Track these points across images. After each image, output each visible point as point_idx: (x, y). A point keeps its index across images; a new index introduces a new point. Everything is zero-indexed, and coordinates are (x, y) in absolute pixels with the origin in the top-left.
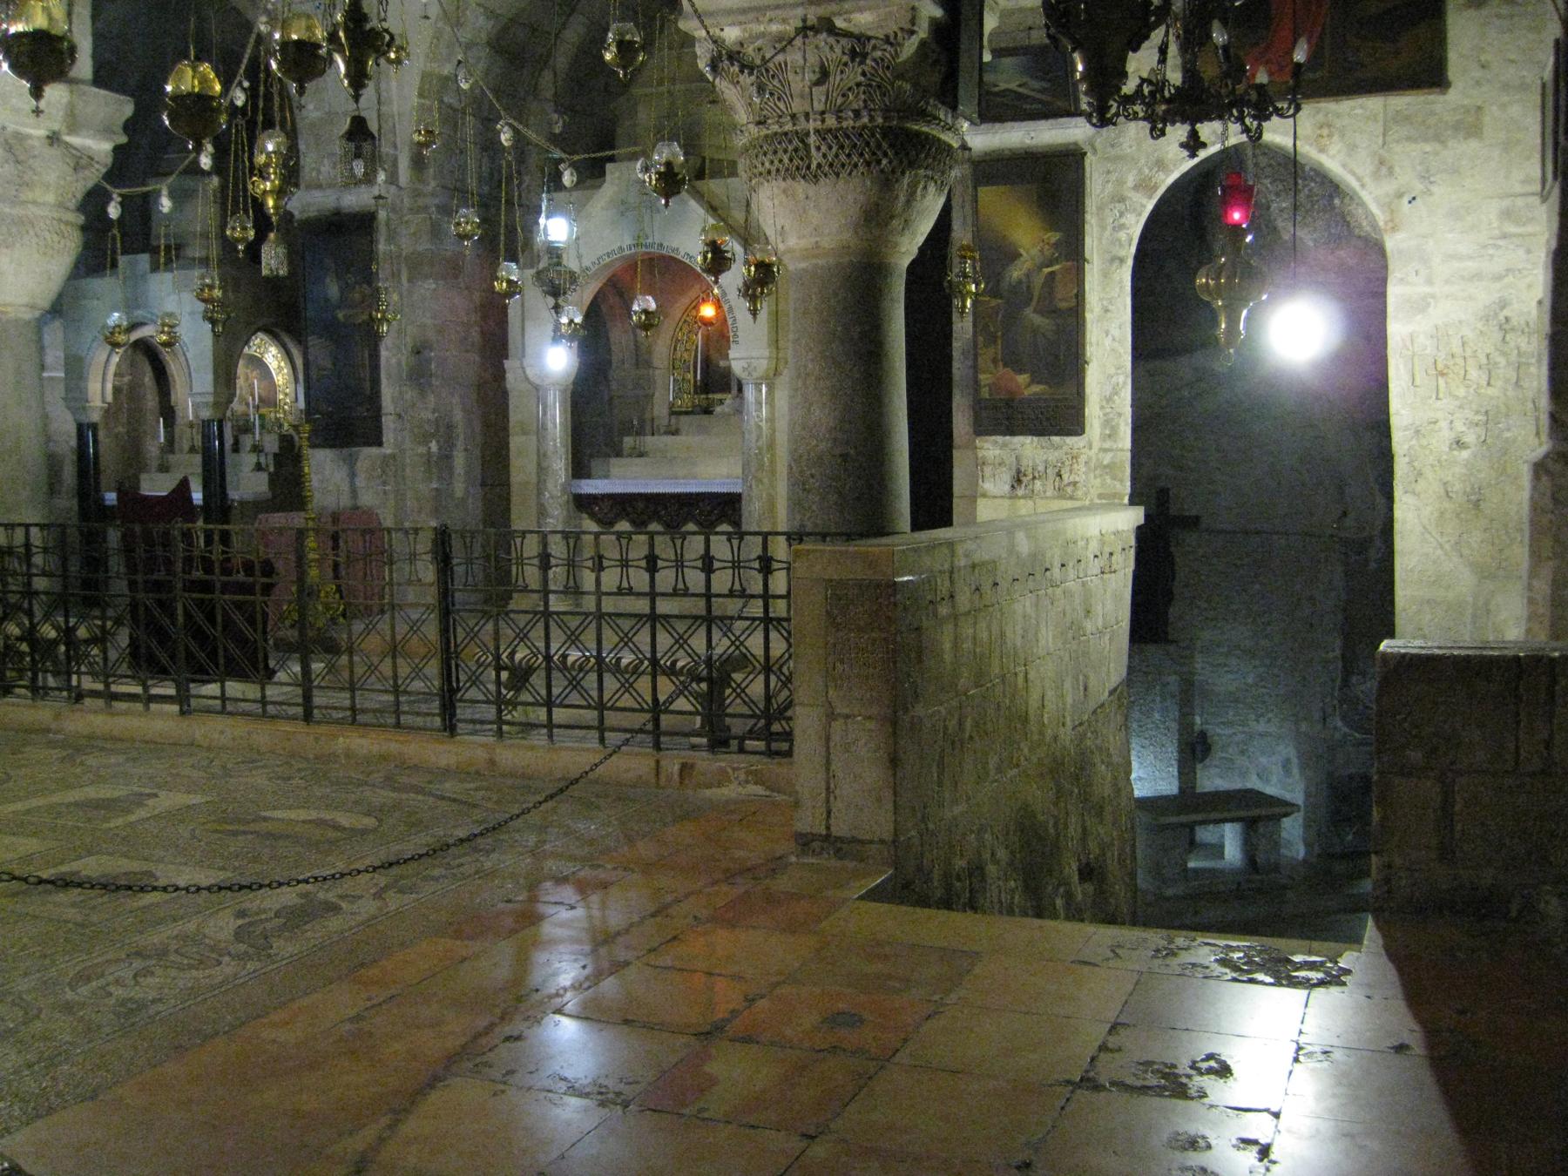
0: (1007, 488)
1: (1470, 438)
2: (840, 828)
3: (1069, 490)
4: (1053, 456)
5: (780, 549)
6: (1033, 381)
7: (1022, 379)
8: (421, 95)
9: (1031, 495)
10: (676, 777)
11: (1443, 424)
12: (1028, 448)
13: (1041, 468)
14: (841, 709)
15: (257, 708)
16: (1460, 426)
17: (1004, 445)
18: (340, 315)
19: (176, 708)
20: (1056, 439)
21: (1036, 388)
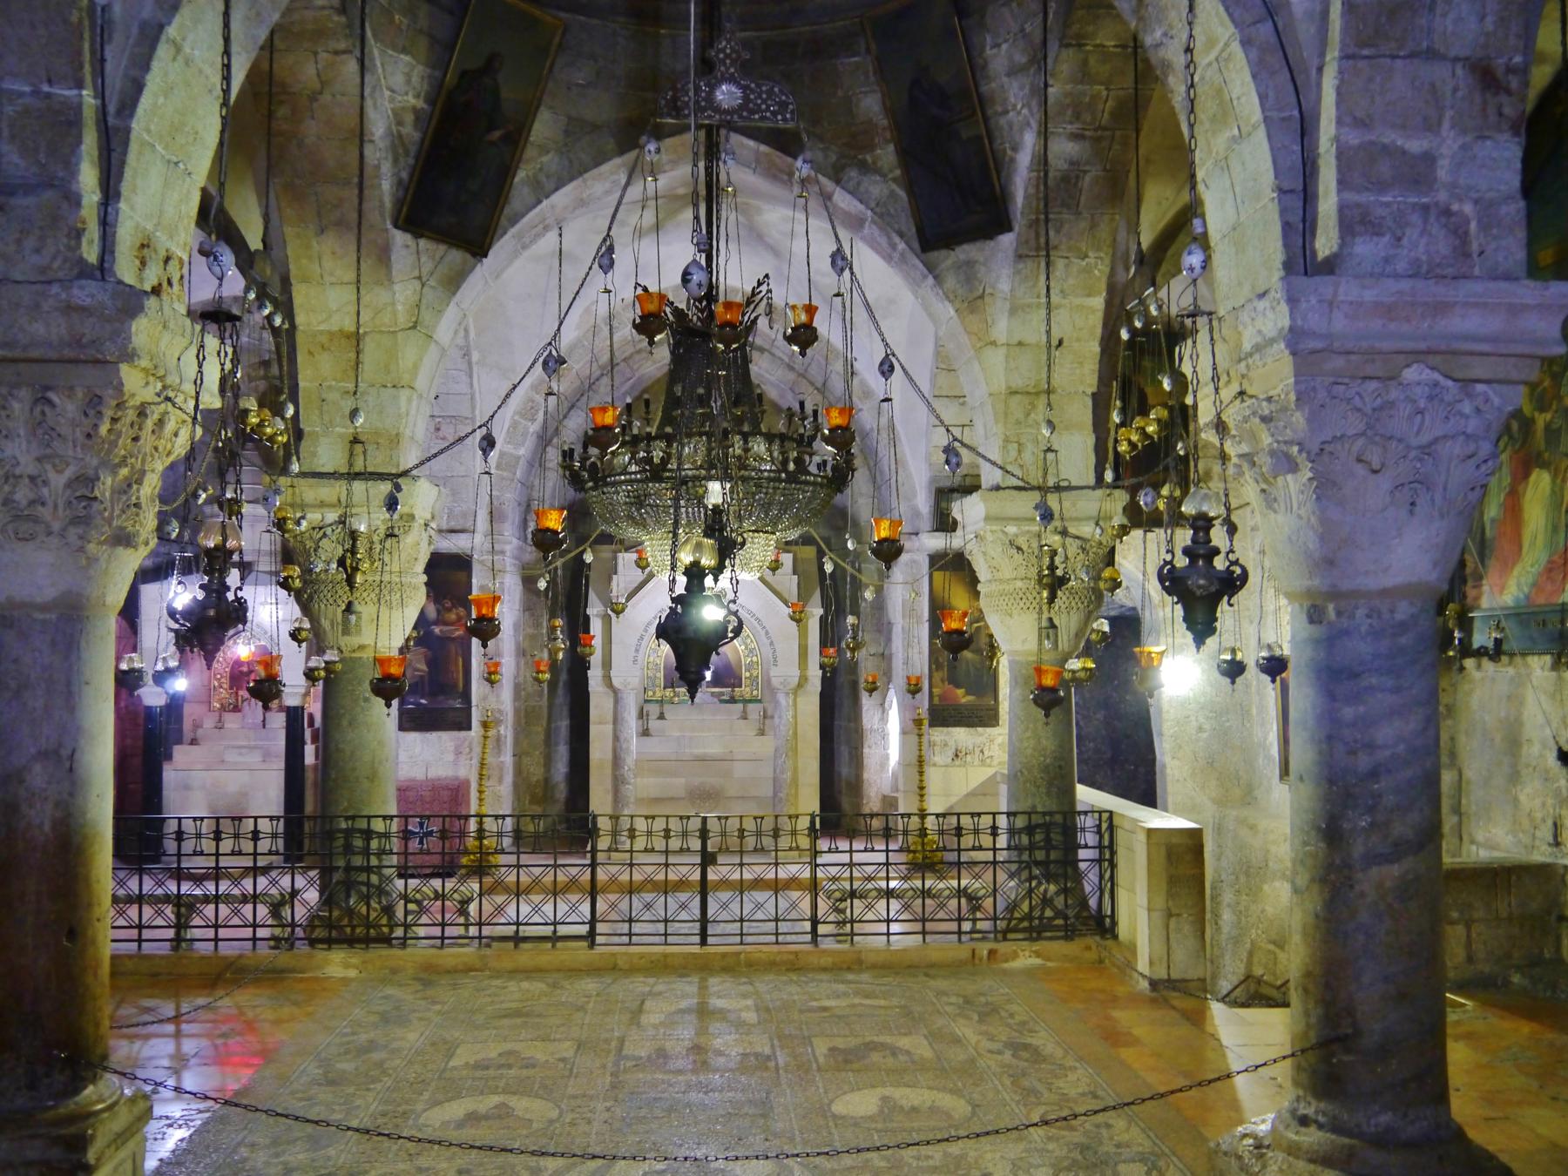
0: (950, 760)
1: (1207, 727)
2: (1174, 976)
3: (988, 761)
4: (979, 740)
5: (1002, 822)
6: (968, 693)
7: (960, 692)
9: (965, 764)
10: (985, 957)
11: (1193, 718)
12: (960, 735)
13: (971, 748)
14: (1174, 911)
15: (773, 938)
16: (1202, 720)
17: (948, 733)
18: (437, 630)
19: (585, 944)
20: (980, 729)
21: (970, 698)
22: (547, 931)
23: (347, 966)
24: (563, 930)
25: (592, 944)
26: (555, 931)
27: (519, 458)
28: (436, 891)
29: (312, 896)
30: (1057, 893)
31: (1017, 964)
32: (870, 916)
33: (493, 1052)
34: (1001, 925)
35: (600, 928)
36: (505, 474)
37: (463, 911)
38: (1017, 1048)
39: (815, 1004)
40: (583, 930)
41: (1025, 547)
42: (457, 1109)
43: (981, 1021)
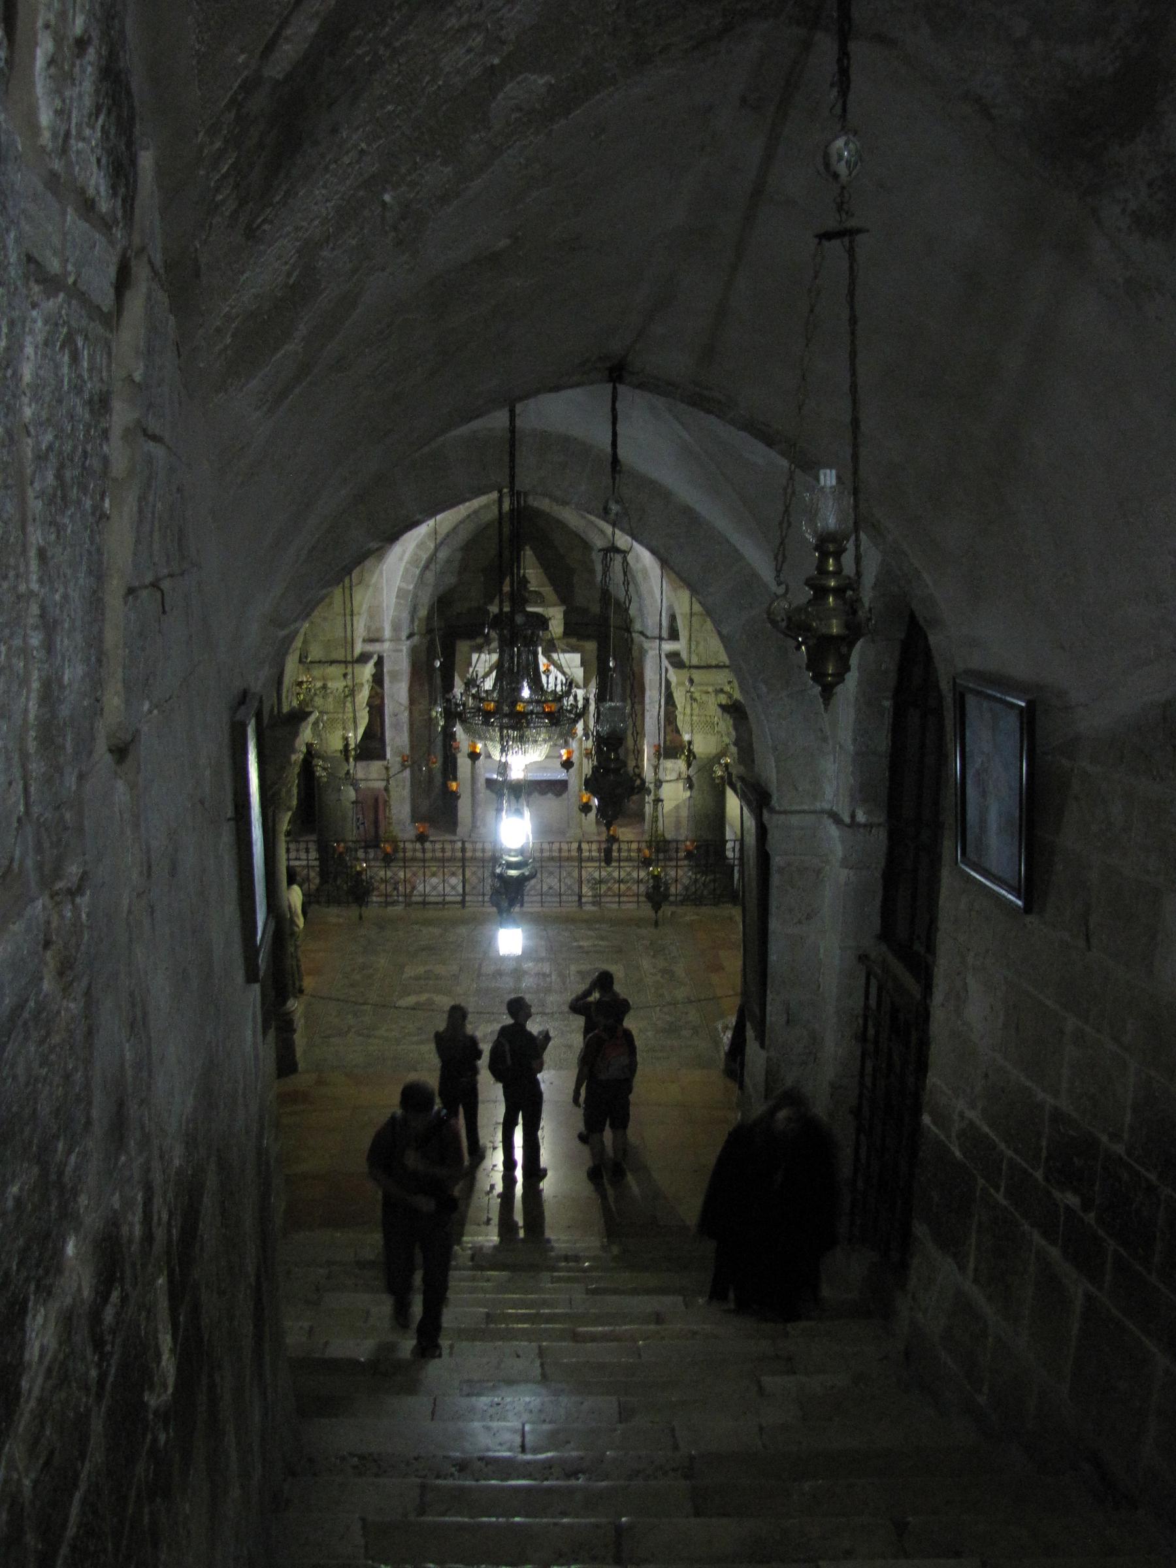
8: (398, 597)
22: (440, 899)
23: (338, 916)
24: (448, 899)
25: (464, 907)
26: (444, 900)
27: (410, 591)
28: (382, 878)
29: (317, 881)
30: (710, 881)
31: (687, 918)
32: (628, 869)
33: (421, 970)
34: (679, 898)
35: (468, 898)
36: (402, 602)
37: (396, 889)
38: (664, 971)
39: (575, 944)
40: (459, 899)
41: (698, 698)
42: (411, 1000)
43: (654, 956)
